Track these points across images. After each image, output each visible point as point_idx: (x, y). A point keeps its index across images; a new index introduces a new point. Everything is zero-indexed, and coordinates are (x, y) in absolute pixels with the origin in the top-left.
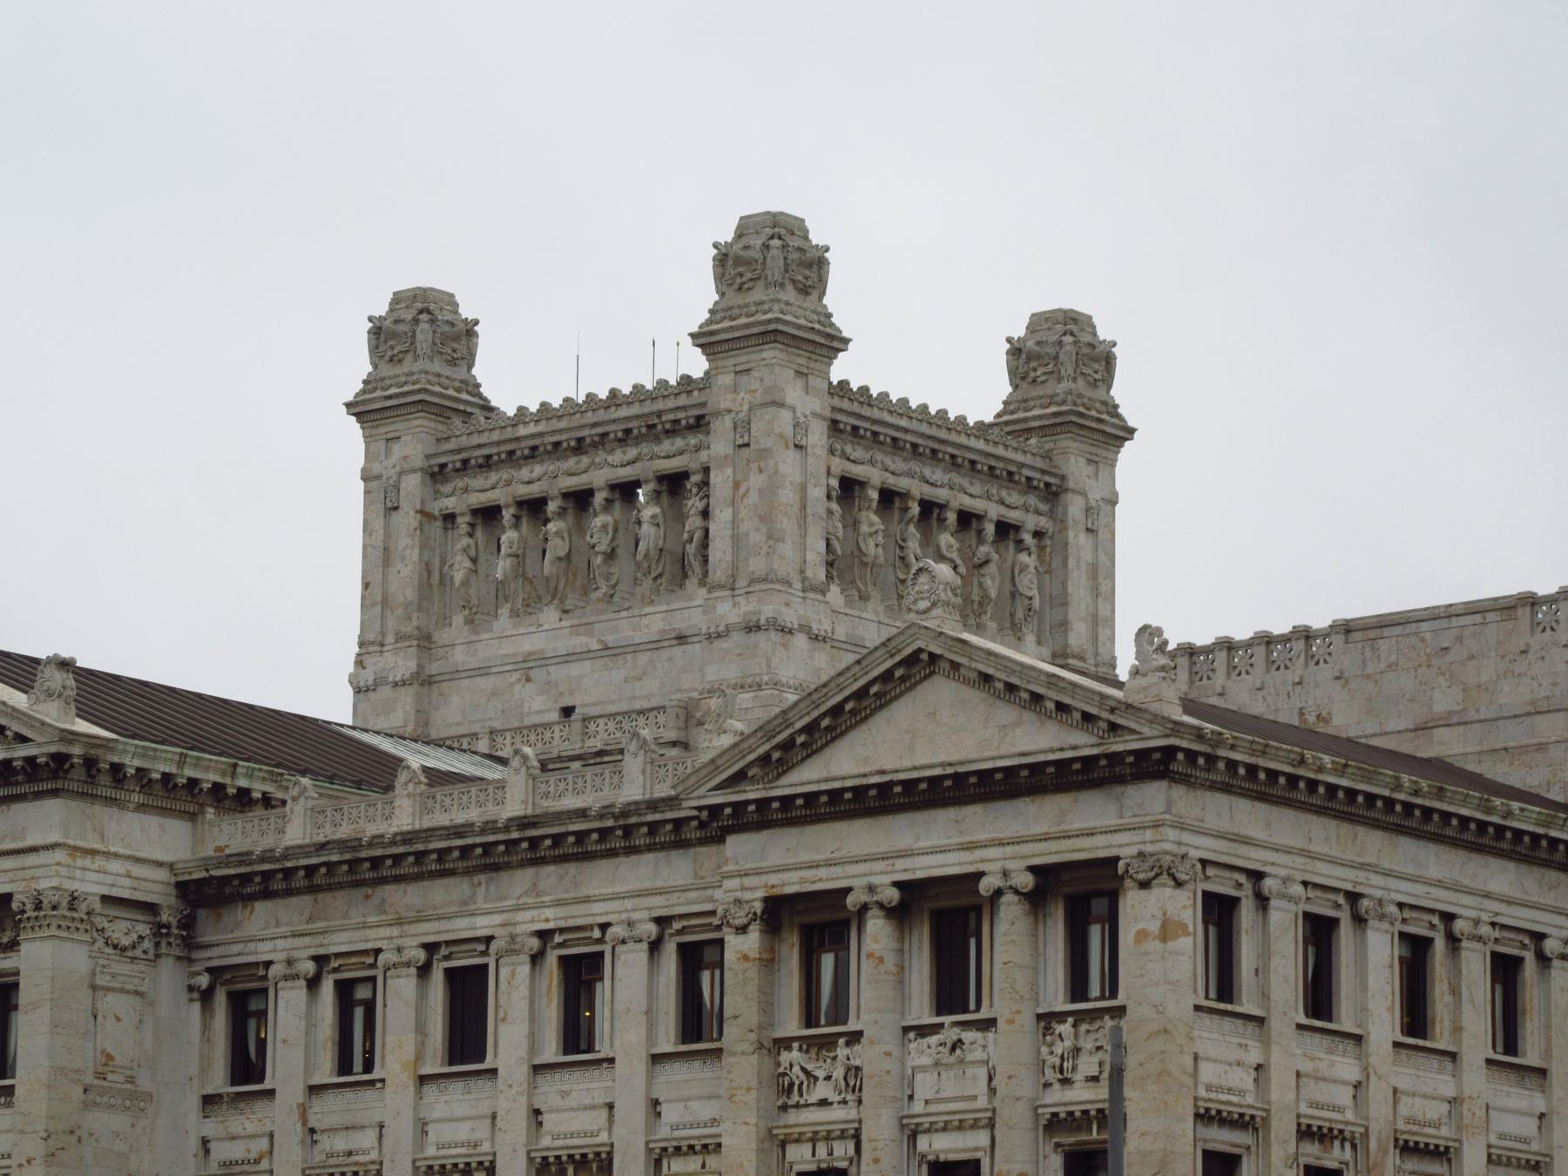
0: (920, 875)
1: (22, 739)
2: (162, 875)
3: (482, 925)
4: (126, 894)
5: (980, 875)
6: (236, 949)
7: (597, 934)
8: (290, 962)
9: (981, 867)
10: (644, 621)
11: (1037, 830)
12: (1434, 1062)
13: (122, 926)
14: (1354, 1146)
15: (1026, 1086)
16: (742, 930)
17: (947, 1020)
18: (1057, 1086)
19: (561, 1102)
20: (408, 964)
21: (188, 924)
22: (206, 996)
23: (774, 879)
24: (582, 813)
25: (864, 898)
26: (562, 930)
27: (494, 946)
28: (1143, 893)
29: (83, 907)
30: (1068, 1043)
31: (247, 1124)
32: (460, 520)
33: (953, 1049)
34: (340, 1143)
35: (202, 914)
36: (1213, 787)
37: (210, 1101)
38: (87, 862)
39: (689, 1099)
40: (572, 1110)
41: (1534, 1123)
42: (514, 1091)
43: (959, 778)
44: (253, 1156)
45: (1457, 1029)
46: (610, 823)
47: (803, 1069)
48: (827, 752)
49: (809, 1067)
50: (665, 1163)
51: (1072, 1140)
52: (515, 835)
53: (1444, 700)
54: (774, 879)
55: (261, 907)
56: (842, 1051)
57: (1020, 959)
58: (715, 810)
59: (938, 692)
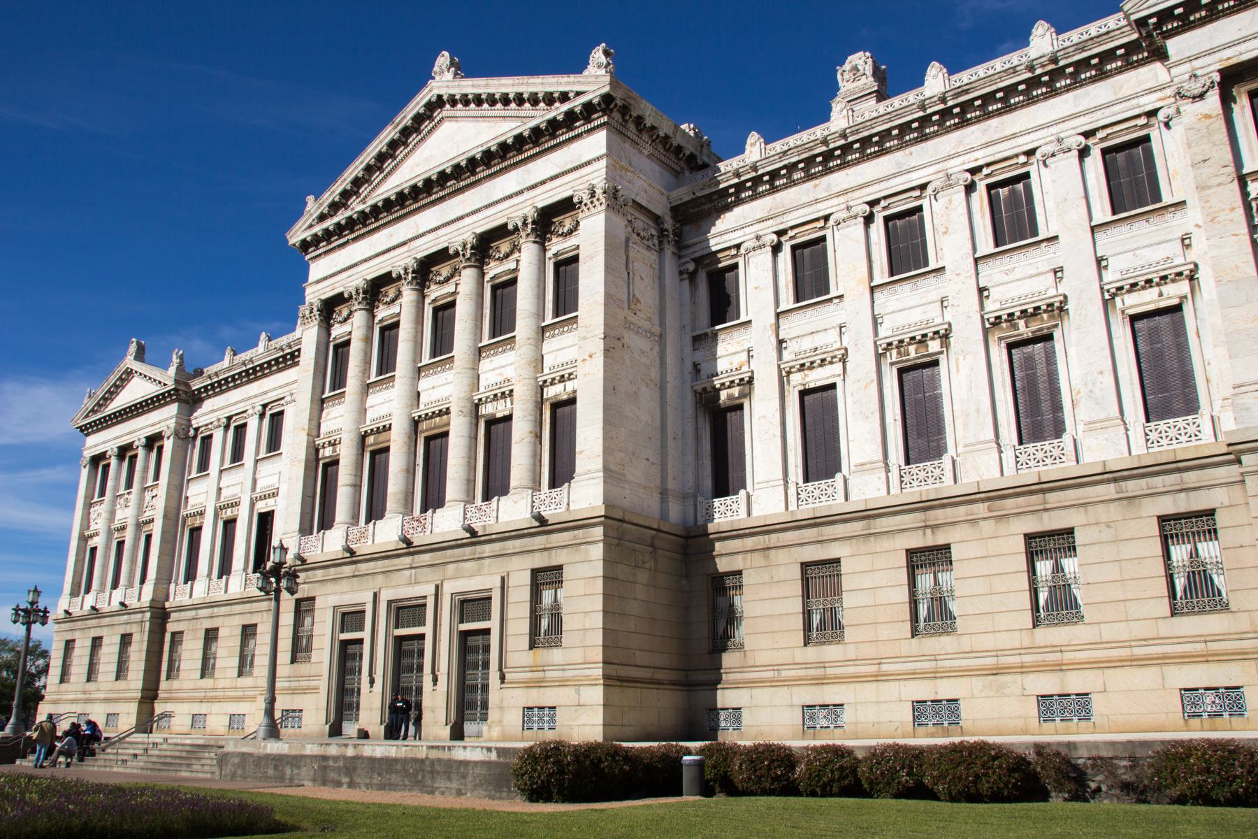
1: (578, 94)
3: (916, 179)
7: (1022, 159)
8: (758, 238)
19: (1006, 278)
20: (855, 217)
21: (678, 234)
22: (692, 276)
31: (729, 347)
34: (807, 344)
35: (687, 228)
39: (1138, 249)
42: (962, 278)
44: (735, 365)
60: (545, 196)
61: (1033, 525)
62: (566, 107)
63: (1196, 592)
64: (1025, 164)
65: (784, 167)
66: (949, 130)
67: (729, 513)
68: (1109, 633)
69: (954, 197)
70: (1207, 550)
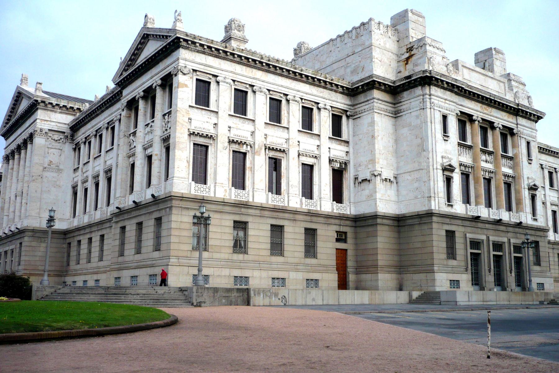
0: (146, 87)
2: (66, 126)
4: (56, 130)
12: (281, 129)
13: (55, 136)
14: (251, 147)
16: (123, 110)
21: (72, 136)
29: (44, 132)
36: (198, 52)
38: (46, 122)
41: (316, 147)
45: (289, 122)
53: (317, 66)
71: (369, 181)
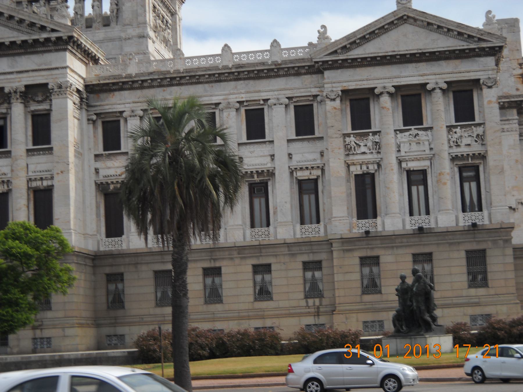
0: (403, 83)
1: (53, 30)
2: (82, 81)
5: (427, 84)
6: (107, 107)
7: (262, 102)
9: (427, 81)
10: (97, 34)
11: (447, 70)
15: (446, 147)
16: (334, 100)
17: (413, 127)
18: (454, 147)
23: (345, 84)
24: (263, 64)
25: (382, 90)
26: (247, 101)
27: (221, 106)
28: (489, 89)
30: (459, 134)
31: (115, 163)
32: (23, 3)
33: (415, 136)
37: (96, 156)
39: (304, 153)
40: (256, 157)
43: (423, 54)
46: (273, 67)
47: (355, 143)
48: (365, 46)
49: (357, 142)
50: (295, 173)
51: (461, 163)
52: (233, 70)
54: (345, 84)
55: (126, 93)
56: (371, 137)
57: (439, 110)
58: (324, 62)
59: (407, 28)
60: (28, 79)
61: (255, 262)
62: (45, 35)
63: (313, 290)
64: (262, 105)
65: (151, 79)
66: (231, 80)
67: (117, 246)
68: (282, 304)
69: (231, 113)
70: (317, 274)
71: (514, 209)
